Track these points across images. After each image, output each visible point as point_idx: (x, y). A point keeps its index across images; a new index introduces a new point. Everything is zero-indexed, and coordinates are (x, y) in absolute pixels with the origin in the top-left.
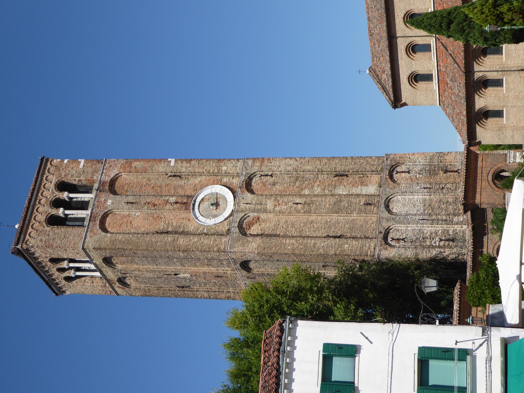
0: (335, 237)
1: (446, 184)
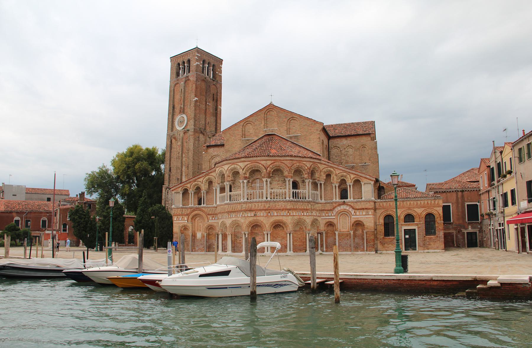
0: (170, 170)
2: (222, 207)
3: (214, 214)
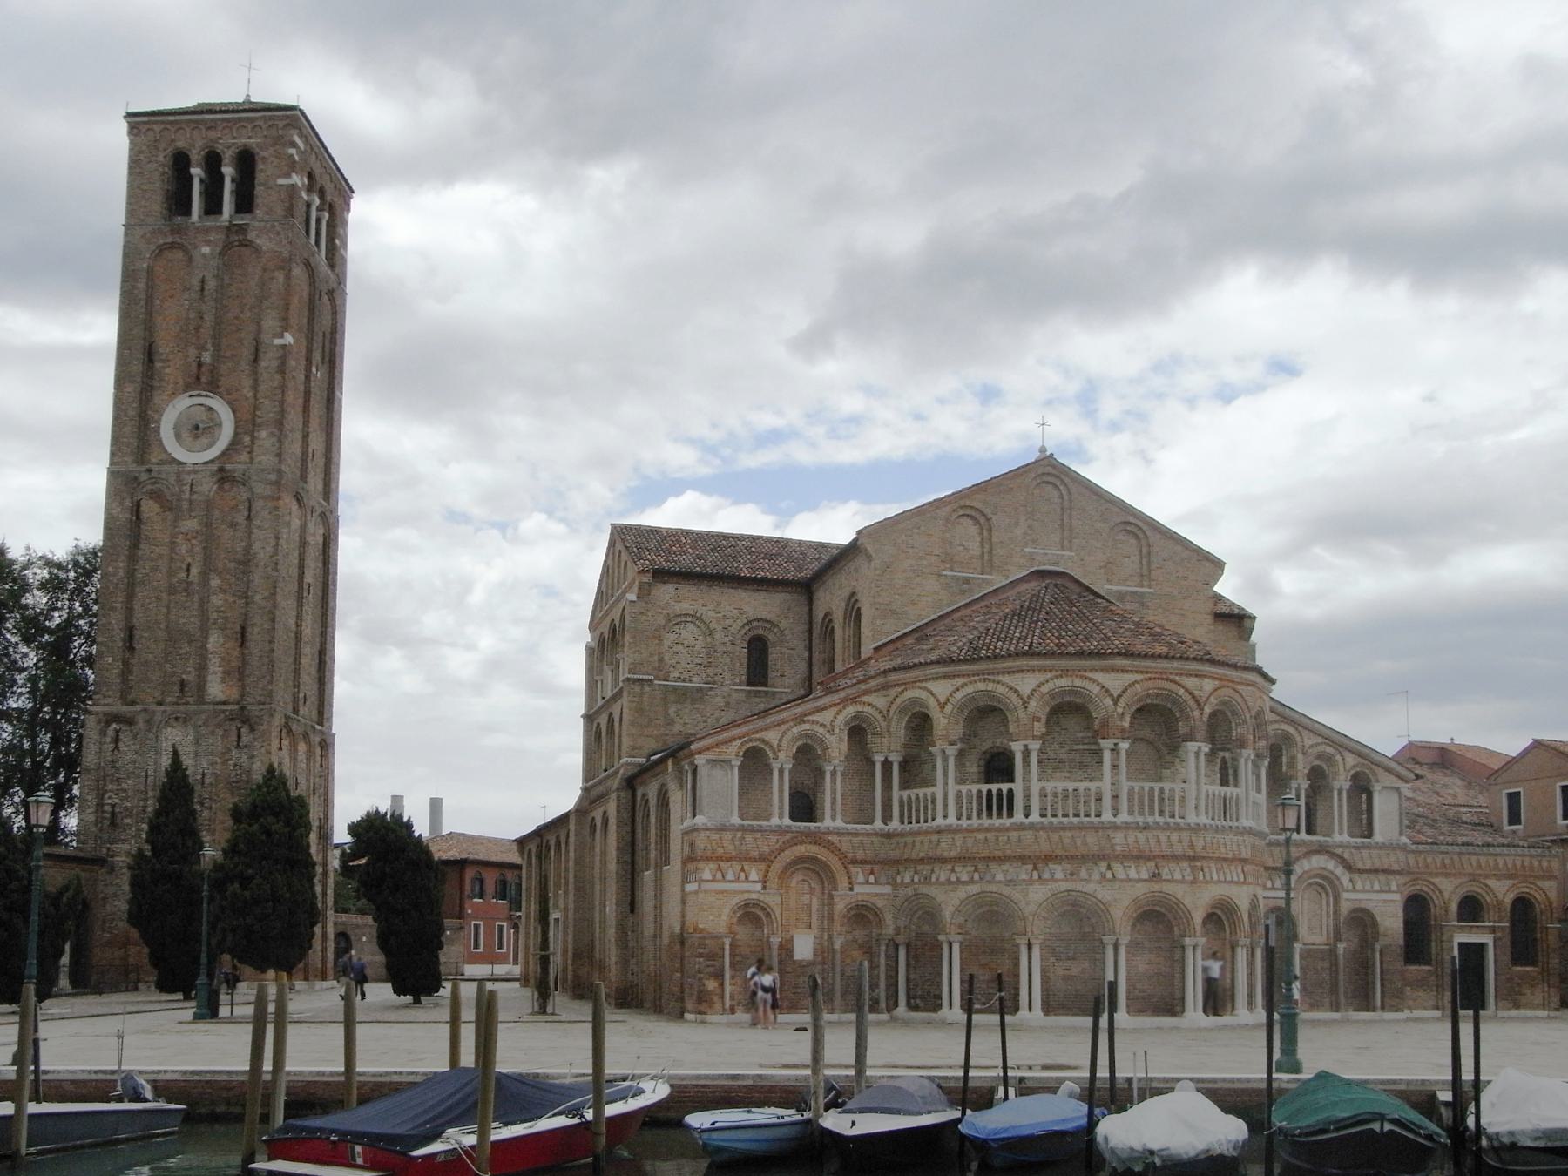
1: (211, 808)
2: (980, 836)
3: (874, 862)
